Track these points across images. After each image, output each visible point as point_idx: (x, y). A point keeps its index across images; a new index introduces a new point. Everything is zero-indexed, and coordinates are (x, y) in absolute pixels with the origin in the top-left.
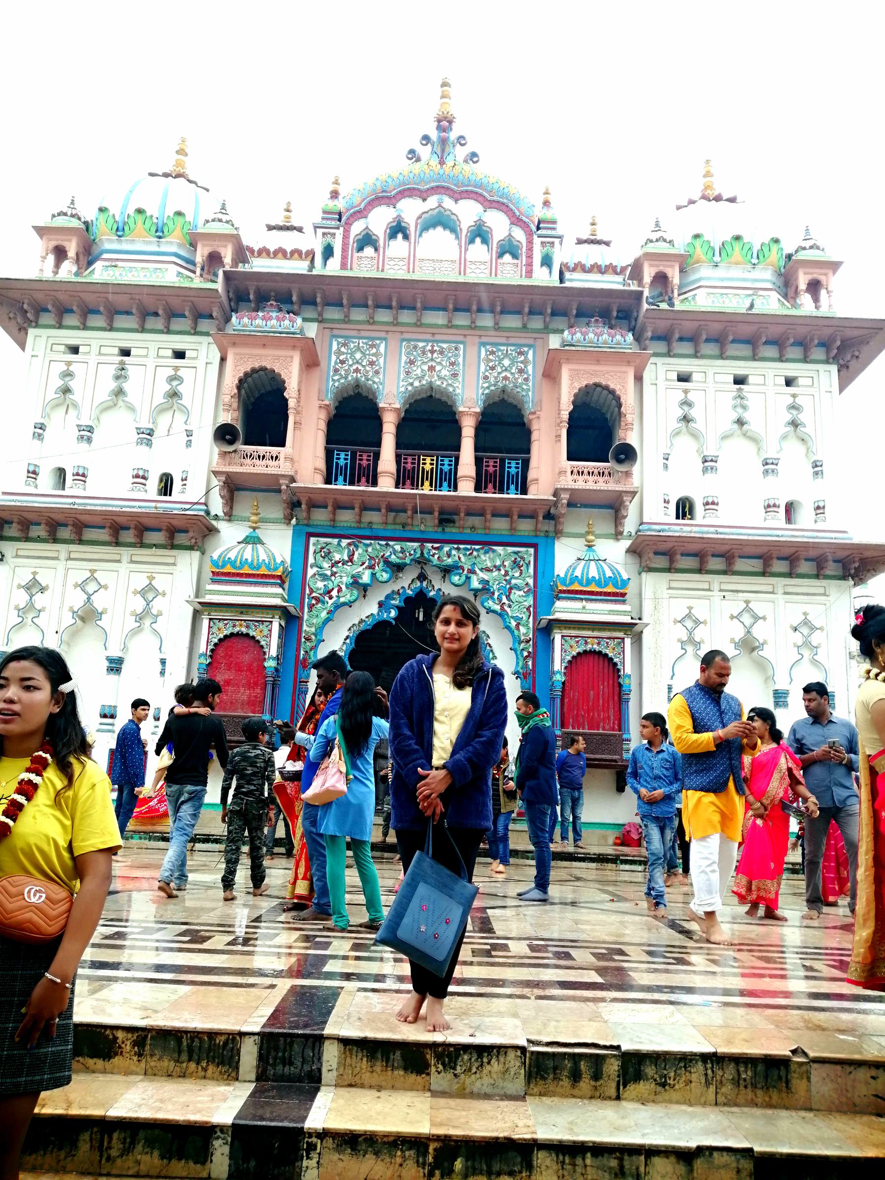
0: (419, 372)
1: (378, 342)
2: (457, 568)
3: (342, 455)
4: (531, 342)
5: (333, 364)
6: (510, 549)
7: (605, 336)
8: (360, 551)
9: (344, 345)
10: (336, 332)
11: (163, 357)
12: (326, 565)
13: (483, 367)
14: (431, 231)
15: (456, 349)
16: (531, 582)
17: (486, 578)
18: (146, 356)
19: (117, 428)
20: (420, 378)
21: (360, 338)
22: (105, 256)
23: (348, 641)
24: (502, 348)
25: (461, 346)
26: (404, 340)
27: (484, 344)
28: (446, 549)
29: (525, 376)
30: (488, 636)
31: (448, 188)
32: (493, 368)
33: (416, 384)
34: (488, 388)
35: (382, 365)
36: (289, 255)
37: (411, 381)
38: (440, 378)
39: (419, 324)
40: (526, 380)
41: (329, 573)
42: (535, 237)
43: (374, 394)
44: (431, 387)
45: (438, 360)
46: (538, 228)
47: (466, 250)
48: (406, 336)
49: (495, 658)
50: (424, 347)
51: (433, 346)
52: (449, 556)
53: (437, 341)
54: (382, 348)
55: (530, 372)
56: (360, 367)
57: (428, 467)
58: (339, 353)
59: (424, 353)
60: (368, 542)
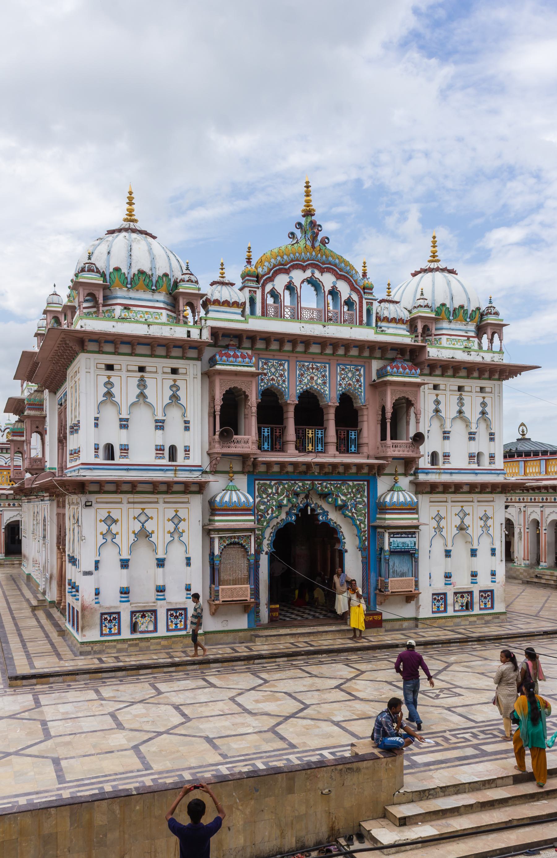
0: (306, 381)
1: (283, 362)
2: (329, 494)
3: (266, 430)
6: (355, 483)
7: (407, 370)
8: (281, 487)
12: (264, 496)
15: (325, 367)
16: (366, 500)
17: (344, 498)
19: (142, 420)
20: (306, 385)
23: (272, 535)
24: (348, 367)
25: (327, 365)
26: (297, 361)
27: (339, 365)
28: (325, 484)
30: (341, 527)
32: (344, 379)
33: (305, 388)
37: (302, 386)
38: (317, 384)
40: (360, 386)
41: (266, 500)
42: (364, 299)
43: (282, 394)
44: (311, 388)
49: (344, 538)
50: (308, 365)
51: (312, 365)
52: (326, 487)
53: (315, 363)
56: (274, 378)
57: (310, 435)
59: (308, 369)
60: (285, 482)
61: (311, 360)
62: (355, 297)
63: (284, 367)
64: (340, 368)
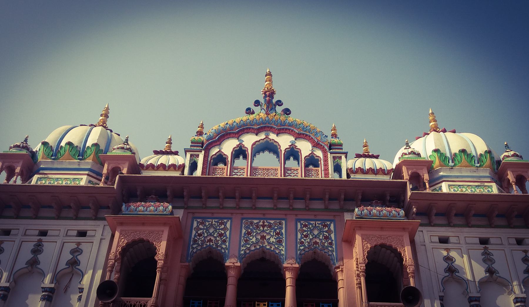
0: (254, 240)
1: (225, 221)
4: (331, 218)
5: (193, 236)
9: (202, 223)
10: (197, 215)
11: (70, 236)
13: (299, 236)
14: (261, 154)
15: (280, 224)
18: (58, 236)
21: (212, 218)
22: (41, 172)
24: (312, 222)
25: (284, 222)
29: (330, 241)
31: (272, 128)
32: (306, 236)
33: (253, 248)
34: (303, 250)
35: (228, 236)
36: (167, 168)
37: (249, 246)
38: (269, 243)
39: (254, 208)
40: (331, 244)
44: (263, 250)
45: (268, 232)
46: (330, 149)
47: (285, 163)
48: (245, 216)
50: (258, 223)
51: (264, 222)
53: (267, 219)
54: (228, 225)
55: (333, 238)
56: (212, 238)
58: (198, 229)
59: (258, 227)
61: (261, 216)
62: (319, 153)
63: (225, 226)
64: (301, 225)
